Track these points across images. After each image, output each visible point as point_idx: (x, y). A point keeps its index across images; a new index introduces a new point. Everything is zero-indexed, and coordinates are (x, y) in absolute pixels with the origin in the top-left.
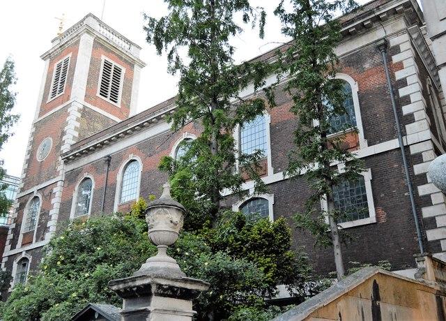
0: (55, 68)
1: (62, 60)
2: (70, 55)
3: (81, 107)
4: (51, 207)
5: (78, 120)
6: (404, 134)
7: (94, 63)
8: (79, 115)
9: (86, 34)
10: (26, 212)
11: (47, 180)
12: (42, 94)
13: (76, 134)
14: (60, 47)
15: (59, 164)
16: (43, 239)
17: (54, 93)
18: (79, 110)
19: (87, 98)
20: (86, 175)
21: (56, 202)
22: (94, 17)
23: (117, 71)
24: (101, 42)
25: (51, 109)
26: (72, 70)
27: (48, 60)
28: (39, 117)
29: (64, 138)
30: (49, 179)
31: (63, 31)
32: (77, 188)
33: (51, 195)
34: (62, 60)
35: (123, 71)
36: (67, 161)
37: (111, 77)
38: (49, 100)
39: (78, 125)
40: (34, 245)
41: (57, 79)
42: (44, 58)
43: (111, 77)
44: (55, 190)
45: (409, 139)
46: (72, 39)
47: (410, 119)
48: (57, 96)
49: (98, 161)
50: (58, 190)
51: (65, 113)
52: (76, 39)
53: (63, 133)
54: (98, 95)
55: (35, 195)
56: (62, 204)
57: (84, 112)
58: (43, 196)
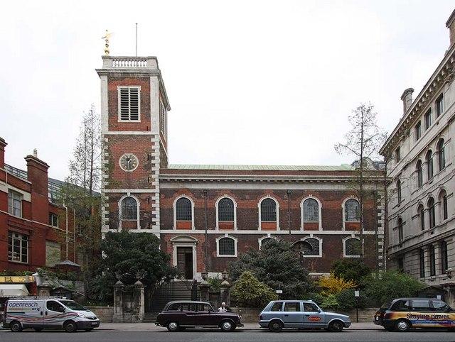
0: (119, 88)
2: (139, 88)
4: (154, 209)
6: (377, 230)
9: (156, 77)
21: (157, 205)
22: (157, 61)
27: (105, 78)
29: (153, 162)
33: (147, 200)
36: (160, 182)
41: (124, 103)
45: (379, 233)
47: (380, 225)
49: (195, 190)
50: (156, 198)
53: (150, 158)
58: (139, 199)
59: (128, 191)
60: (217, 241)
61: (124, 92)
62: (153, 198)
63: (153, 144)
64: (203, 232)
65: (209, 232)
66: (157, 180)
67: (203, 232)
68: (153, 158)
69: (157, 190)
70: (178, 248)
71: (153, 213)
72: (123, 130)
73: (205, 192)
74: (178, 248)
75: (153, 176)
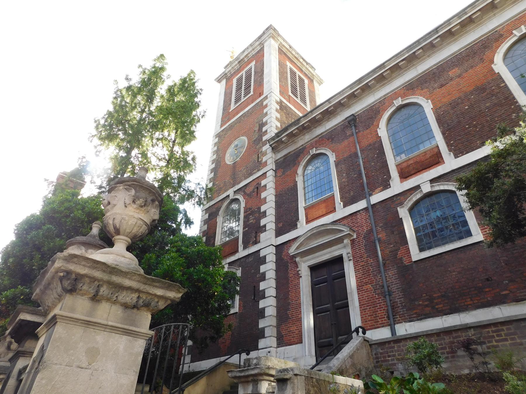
0: (235, 81)
1: (243, 72)
3: (279, 100)
4: (264, 201)
5: (277, 110)
7: (282, 67)
8: (278, 107)
10: (220, 220)
11: (246, 178)
12: (222, 107)
13: (279, 125)
14: (239, 62)
15: (265, 154)
16: (256, 242)
17: (238, 99)
18: (277, 103)
19: (281, 93)
20: (314, 151)
23: (302, 81)
24: (284, 50)
25: (237, 113)
26: (260, 72)
27: (224, 82)
28: (221, 126)
29: (264, 129)
30: (251, 174)
31: (235, 58)
32: (300, 171)
34: (243, 72)
35: (306, 81)
36: (275, 149)
37: (298, 83)
38: (233, 107)
39: (278, 116)
40: (242, 253)
42: (219, 80)
43: (298, 83)
44: (263, 183)
46: (253, 49)
48: (242, 100)
51: (261, 106)
52: (259, 48)
54: (290, 94)
55: (231, 197)
56: (279, 196)
57: (282, 107)
58: (245, 195)
59: (230, 192)
60: (403, 213)
61: (239, 81)
62: (263, 183)
63: (266, 106)
64: (361, 205)
65: (377, 198)
66: (270, 150)
67: (361, 205)
68: (266, 123)
69: (271, 165)
70: (313, 269)
71: (263, 209)
72: (234, 116)
73: (352, 121)
74: (313, 269)
75: (264, 149)
